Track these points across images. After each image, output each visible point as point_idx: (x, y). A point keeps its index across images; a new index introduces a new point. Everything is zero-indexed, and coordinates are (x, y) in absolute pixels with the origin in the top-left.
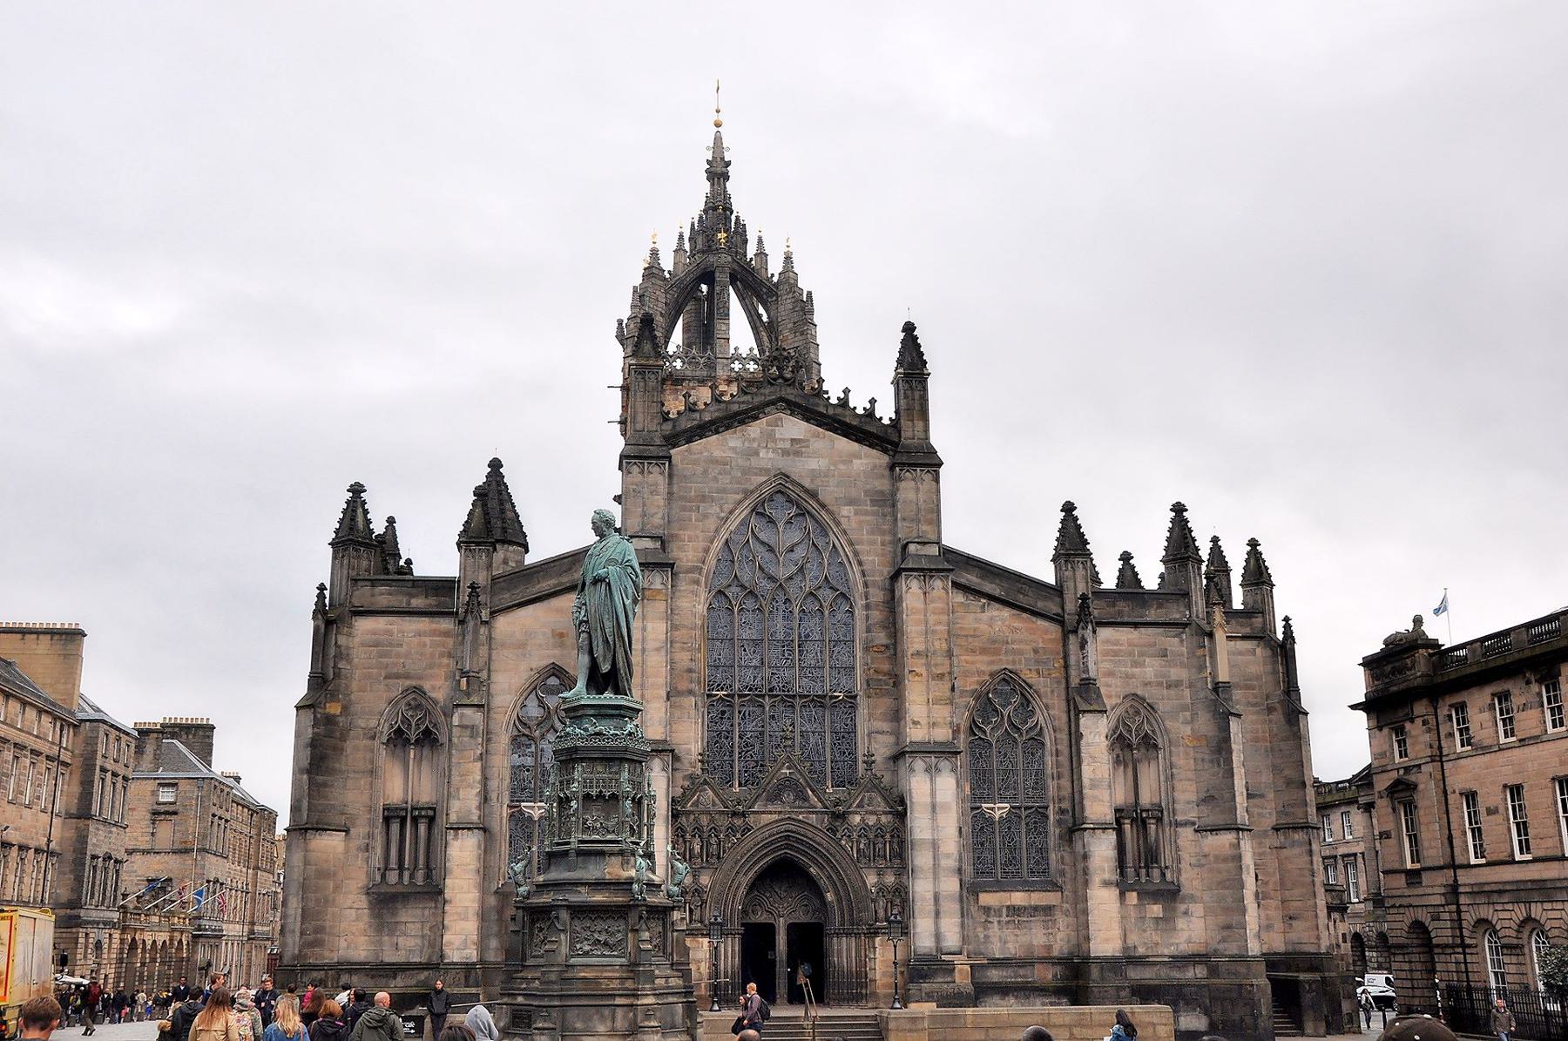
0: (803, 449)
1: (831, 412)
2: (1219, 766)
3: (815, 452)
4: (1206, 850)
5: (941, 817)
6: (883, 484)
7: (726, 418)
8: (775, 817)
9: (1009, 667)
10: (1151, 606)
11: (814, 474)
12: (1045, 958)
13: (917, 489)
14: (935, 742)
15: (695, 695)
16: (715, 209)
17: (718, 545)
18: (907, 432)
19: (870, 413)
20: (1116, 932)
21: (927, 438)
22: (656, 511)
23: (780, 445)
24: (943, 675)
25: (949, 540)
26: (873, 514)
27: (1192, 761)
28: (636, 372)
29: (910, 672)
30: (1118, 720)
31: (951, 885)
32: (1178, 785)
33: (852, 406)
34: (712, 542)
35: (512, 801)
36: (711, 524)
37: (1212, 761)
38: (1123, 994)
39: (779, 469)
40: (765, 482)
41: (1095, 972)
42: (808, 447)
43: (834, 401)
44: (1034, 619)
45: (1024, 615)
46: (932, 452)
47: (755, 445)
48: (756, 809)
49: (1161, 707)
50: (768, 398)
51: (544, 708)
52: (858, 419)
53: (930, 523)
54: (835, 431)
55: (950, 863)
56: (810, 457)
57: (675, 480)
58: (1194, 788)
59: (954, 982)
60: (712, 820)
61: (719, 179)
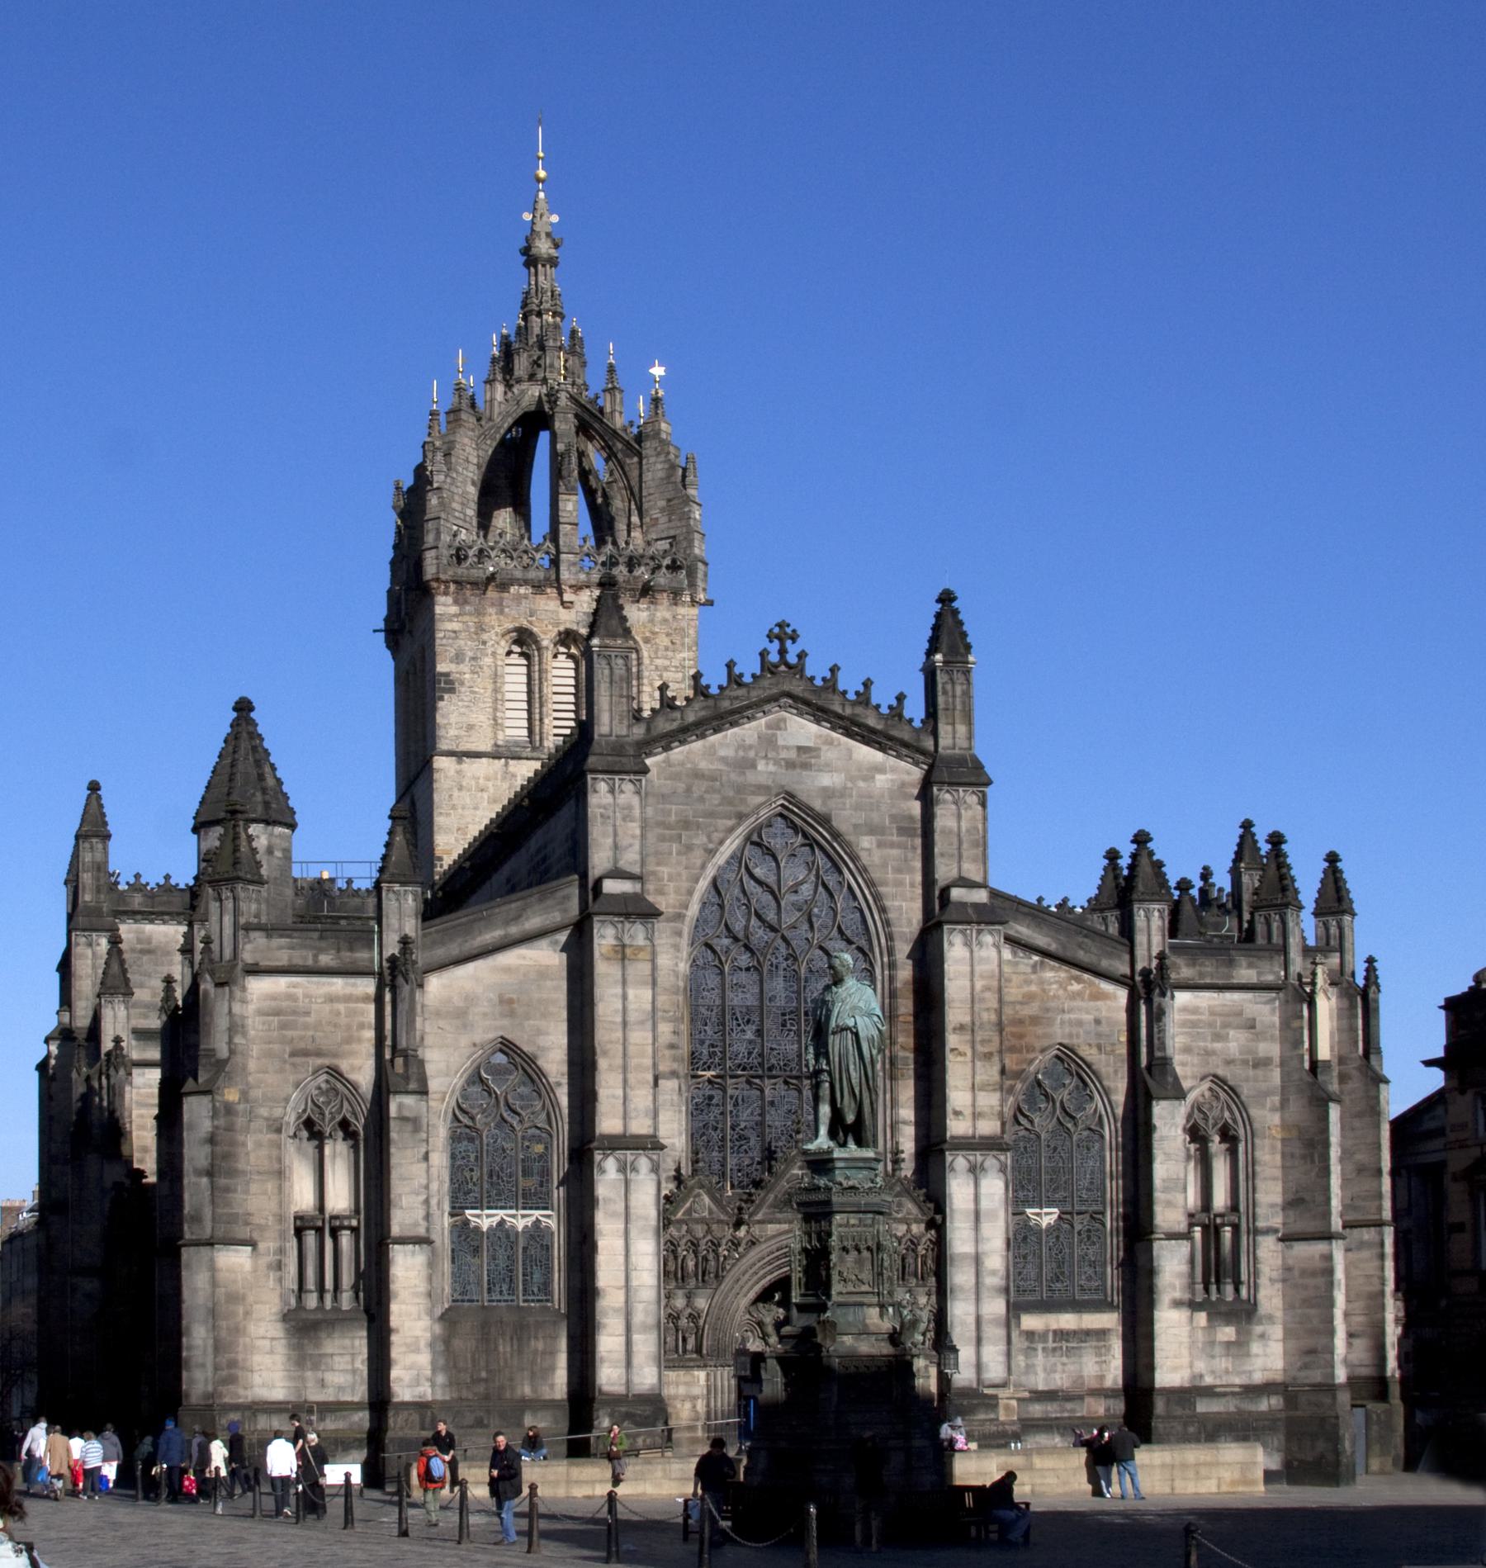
0: (813, 761)
1: (848, 711)
2: (1313, 1161)
3: (827, 765)
4: (1290, 1262)
5: (987, 1228)
6: (916, 808)
7: (715, 718)
8: (785, 1227)
9: (1065, 1041)
10: (1240, 966)
11: (828, 793)
12: (1096, 1390)
13: (959, 817)
14: (981, 1137)
15: (678, 1077)
17: (704, 884)
18: (945, 741)
19: (896, 712)
20: (1185, 1360)
21: (970, 749)
22: (631, 841)
23: (784, 755)
24: (991, 1054)
25: (993, 884)
26: (899, 846)
27: (1278, 1157)
29: (952, 1050)
30: (1192, 1107)
31: (996, 1307)
32: (1260, 1184)
33: (874, 701)
34: (697, 881)
35: (453, 1208)
36: (697, 857)
37: (1304, 1157)
38: (1191, 1429)
39: (783, 787)
41: (1160, 1406)
42: (818, 757)
43: (851, 696)
44: (1096, 981)
45: (1086, 976)
46: (978, 767)
47: (752, 754)
48: (759, 1217)
49: (1246, 1091)
50: (768, 693)
51: (490, 1094)
53: (975, 860)
54: (849, 734)
55: (994, 1280)
56: (821, 771)
57: (651, 800)
58: (1278, 1187)
59: (997, 1419)
60: (709, 1231)
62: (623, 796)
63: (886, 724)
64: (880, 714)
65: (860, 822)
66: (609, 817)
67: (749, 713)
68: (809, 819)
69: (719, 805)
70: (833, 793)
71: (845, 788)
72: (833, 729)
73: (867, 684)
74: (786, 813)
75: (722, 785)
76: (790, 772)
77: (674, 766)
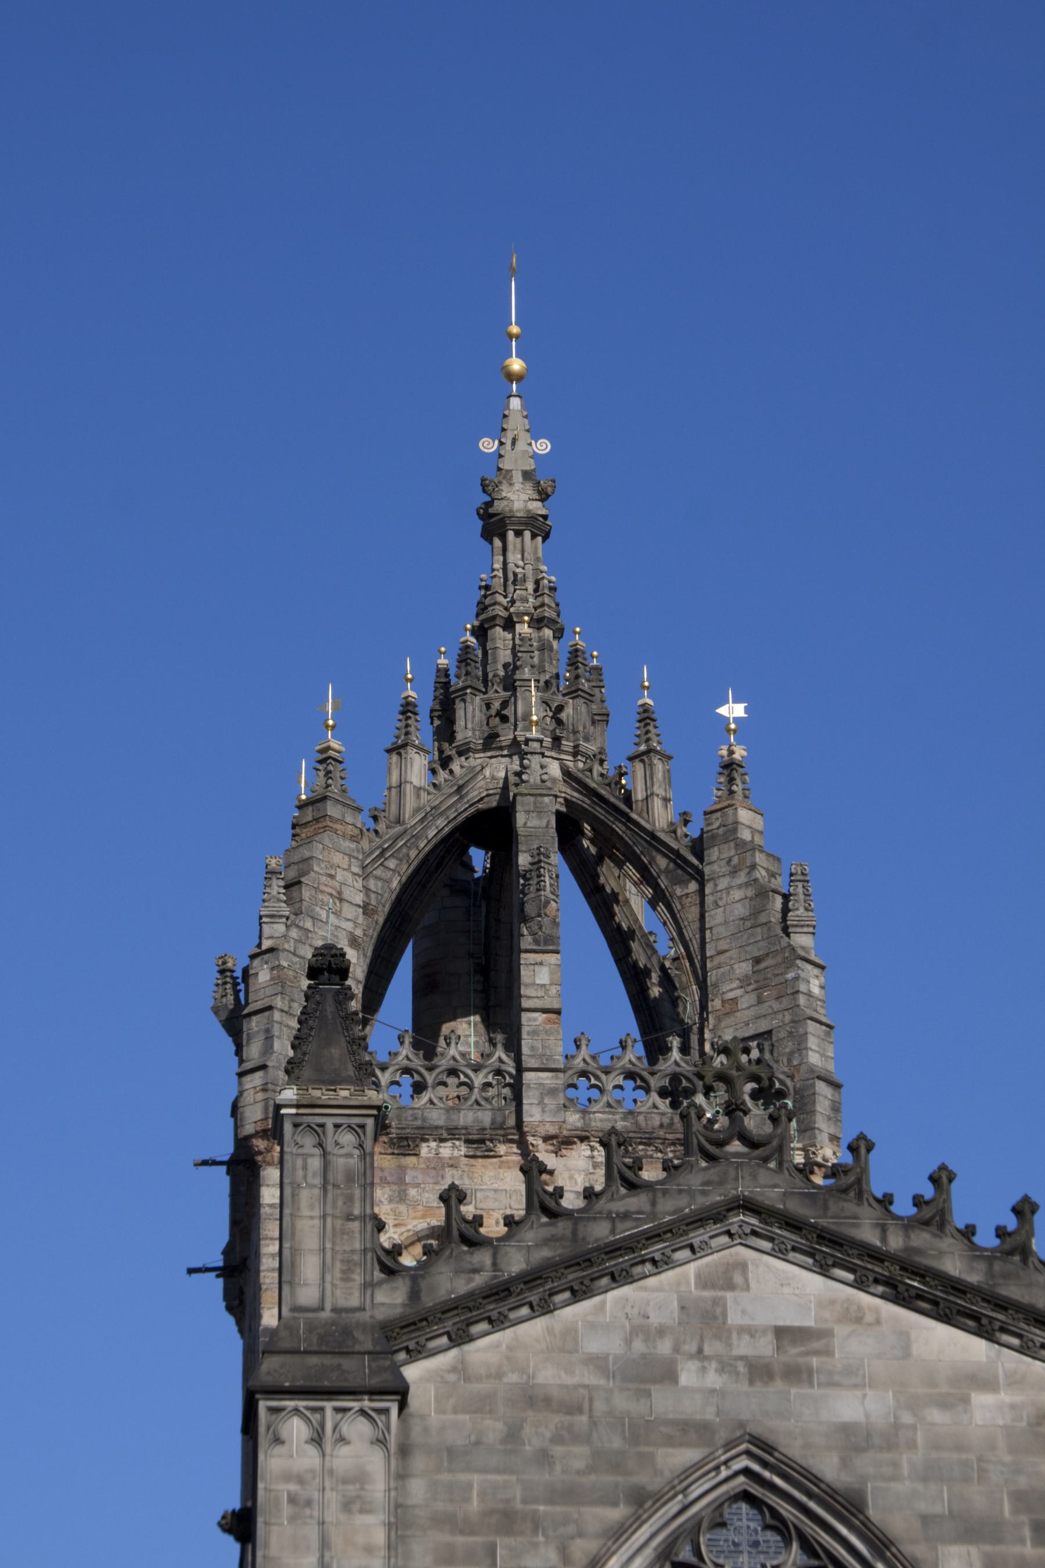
0: (815, 1361)
1: (895, 1242)
3: (849, 1371)
16: (509, 625)
23: (743, 1347)
28: (296, 1126)
33: (959, 1220)
39: (741, 1425)
40: (697, 1466)
42: (828, 1352)
43: (903, 1207)
47: (664, 1347)
52: (982, 1266)
57: (419, 1462)
61: (519, 533)
62: (344, 1450)
63: (990, 1273)
64: (973, 1246)
65: (937, 1509)
66: (309, 1503)
67: (655, 1250)
68: (812, 1505)
69: (591, 1469)
70: (869, 1435)
71: (897, 1426)
72: (859, 1285)
73: (941, 1178)
74: (757, 1490)
75: (593, 1423)
76: (759, 1387)
77: (479, 1379)
